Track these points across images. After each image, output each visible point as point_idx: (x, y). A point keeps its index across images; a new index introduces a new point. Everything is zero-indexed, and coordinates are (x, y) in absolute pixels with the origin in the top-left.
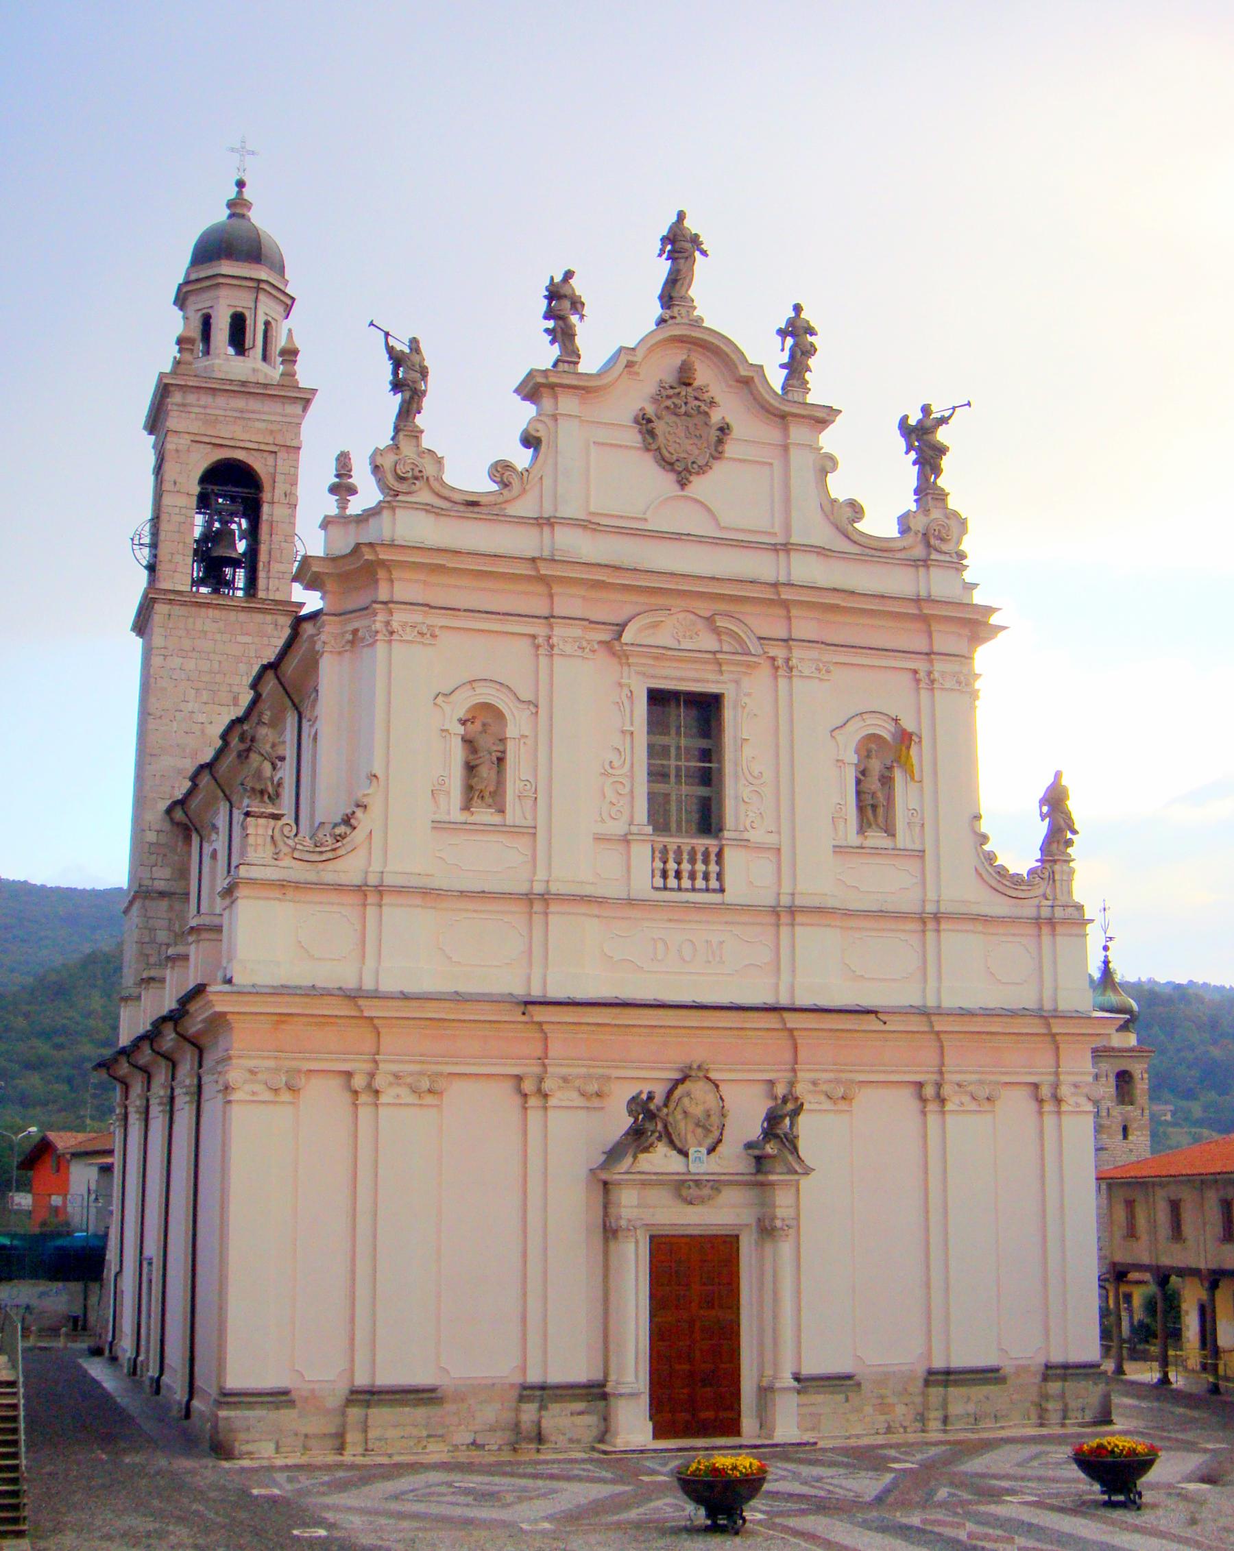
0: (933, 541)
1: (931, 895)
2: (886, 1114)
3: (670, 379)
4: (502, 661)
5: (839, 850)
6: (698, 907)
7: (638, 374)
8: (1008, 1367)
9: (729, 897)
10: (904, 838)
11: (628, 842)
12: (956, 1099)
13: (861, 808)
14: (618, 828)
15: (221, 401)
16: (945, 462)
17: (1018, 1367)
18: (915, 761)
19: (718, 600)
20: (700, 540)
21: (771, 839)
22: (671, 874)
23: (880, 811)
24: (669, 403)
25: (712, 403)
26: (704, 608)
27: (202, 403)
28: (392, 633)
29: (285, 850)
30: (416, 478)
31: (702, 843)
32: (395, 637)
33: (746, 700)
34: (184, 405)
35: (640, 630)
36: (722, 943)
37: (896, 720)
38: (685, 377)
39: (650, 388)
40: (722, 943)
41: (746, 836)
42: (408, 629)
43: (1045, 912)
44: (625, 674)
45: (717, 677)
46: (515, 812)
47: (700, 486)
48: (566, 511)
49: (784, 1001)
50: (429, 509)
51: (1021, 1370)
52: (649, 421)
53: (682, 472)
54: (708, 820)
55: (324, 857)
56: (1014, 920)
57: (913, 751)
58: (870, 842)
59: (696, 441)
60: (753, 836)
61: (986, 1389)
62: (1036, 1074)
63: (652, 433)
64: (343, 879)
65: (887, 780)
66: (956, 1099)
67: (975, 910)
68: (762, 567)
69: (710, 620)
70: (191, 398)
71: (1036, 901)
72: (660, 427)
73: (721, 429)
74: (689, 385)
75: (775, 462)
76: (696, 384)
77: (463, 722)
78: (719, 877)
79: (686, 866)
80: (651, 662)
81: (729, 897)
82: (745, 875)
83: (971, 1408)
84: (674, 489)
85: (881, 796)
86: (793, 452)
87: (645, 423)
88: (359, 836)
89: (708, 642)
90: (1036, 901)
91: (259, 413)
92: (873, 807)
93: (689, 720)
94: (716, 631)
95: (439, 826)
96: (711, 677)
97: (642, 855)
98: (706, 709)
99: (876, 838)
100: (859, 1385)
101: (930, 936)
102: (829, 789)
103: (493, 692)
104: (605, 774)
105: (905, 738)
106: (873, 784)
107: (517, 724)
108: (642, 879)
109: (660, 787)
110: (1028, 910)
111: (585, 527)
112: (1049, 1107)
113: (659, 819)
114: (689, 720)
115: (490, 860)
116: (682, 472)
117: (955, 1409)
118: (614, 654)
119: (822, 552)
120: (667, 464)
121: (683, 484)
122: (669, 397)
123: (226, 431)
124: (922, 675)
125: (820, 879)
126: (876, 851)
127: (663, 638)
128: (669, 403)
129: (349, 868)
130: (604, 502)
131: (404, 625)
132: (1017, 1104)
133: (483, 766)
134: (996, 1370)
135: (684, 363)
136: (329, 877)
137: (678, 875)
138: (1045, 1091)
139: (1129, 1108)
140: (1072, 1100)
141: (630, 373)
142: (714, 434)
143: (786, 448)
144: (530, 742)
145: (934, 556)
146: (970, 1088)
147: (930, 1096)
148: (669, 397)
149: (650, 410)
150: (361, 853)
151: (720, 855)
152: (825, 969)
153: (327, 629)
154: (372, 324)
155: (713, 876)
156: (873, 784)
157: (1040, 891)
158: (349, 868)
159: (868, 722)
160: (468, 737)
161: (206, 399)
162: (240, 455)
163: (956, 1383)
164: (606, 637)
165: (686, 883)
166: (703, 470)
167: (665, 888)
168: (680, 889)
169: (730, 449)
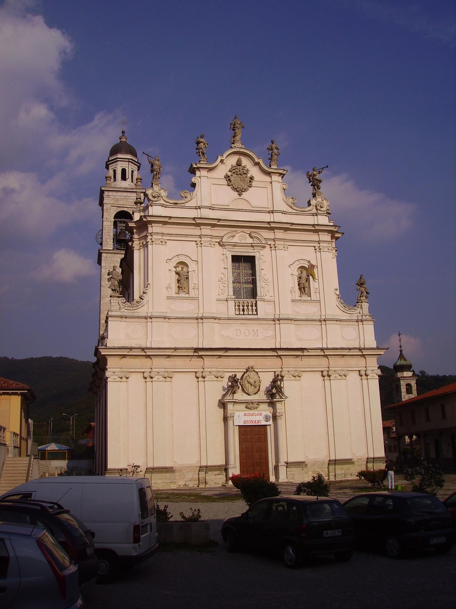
0: (318, 208)
1: (323, 313)
2: (312, 381)
3: (234, 164)
4: (188, 249)
5: (293, 301)
6: (249, 319)
7: (225, 163)
8: (355, 459)
9: (259, 316)
10: (314, 297)
11: (227, 301)
12: (334, 375)
13: (300, 289)
14: (224, 297)
15: (119, 194)
16: (321, 185)
17: (358, 459)
18: (316, 273)
19: (252, 227)
20: (246, 211)
21: (272, 299)
22: (241, 310)
23: (306, 289)
24: (234, 171)
25: (247, 170)
26: (248, 231)
27: (114, 195)
28: (152, 242)
29: (123, 307)
30: (158, 197)
31: (251, 301)
32: (154, 243)
33: (262, 257)
34: (108, 196)
35: (228, 238)
36: (257, 330)
37: (309, 261)
38: (239, 163)
39: (229, 167)
40: (257, 330)
41: (264, 298)
42: (157, 241)
43: (360, 318)
44: (225, 251)
45: (253, 251)
46: (193, 293)
47: (245, 195)
48: (205, 204)
49: (278, 347)
50: (162, 206)
51: (359, 459)
52: (229, 177)
53: (240, 191)
54: (253, 294)
55: (134, 308)
56: (350, 321)
57: (315, 270)
58: (303, 298)
59: (243, 182)
60: (266, 298)
61: (348, 466)
62: (359, 367)
63: (230, 180)
64: (140, 315)
65: (307, 280)
66: (334, 375)
67: (337, 317)
68: (267, 218)
69: (250, 235)
70: (110, 193)
71: (357, 315)
72: (232, 178)
73: (251, 178)
74: (241, 165)
75: (268, 187)
76: (242, 165)
77: (175, 267)
78: (256, 310)
79: (245, 308)
80: (232, 247)
81: (259, 316)
82: (264, 310)
83: (343, 472)
84: (238, 197)
85: (306, 285)
86: (273, 183)
87: (227, 177)
88: (144, 301)
89: (250, 241)
90: (357, 315)
91: (131, 197)
92: (303, 288)
93: (245, 262)
94: (251, 237)
95: (168, 298)
96: (250, 251)
97: (231, 304)
98: (251, 260)
99: (305, 297)
100: (307, 465)
101: (324, 326)
102: (291, 283)
103: (184, 258)
104: (219, 281)
105: (312, 266)
106: (303, 281)
107: (192, 267)
108: (232, 312)
109: (237, 285)
110: (355, 318)
111: (210, 209)
112: (364, 377)
113: (237, 293)
114: (245, 262)
115: (185, 307)
116: (240, 191)
117: (338, 472)
118: (221, 246)
119: (283, 213)
120: (235, 189)
121: (240, 195)
122: (234, 169)
123: (121, 203)
124: (317, 248)
125: (288, 310)
126: (305, 301)
127: (236, 240)
128: (234, 171)
129: (142, 311)
130: (215, 201)
131: (156, 239)
132: (354, 377)
133: (182, 280)
134: (351, 460)
135: (238, 159)
136: (136, 314)
137: (243, 310)
138: (363, 373)
139: (410, 395)
140: (371, 375)
141: (222, 164)
142: (249, 180)
143: (271, 183)
144: (196, 272)
145: (319, 212)
146: (338, 372)
147: (326, 375)
148: (234, 169)
149: (229, 174)
150: (146, 306)
151: (256, 304)
152: (290, 337)
153: (135, 243)
154: (143, 153)
155: (254, 310)
156: (303, 281)
157: (358, 311)
158: (142, 311)
159: (301, 262)
160: (177, 272)
161: (115, 193)
162: (125, 209)
163: (339, 464)
164: (218, 240)
165: (246, 313)
166: (246, 190)
167: (240, 314)
168: (244, 314)
169: (254, 184)
